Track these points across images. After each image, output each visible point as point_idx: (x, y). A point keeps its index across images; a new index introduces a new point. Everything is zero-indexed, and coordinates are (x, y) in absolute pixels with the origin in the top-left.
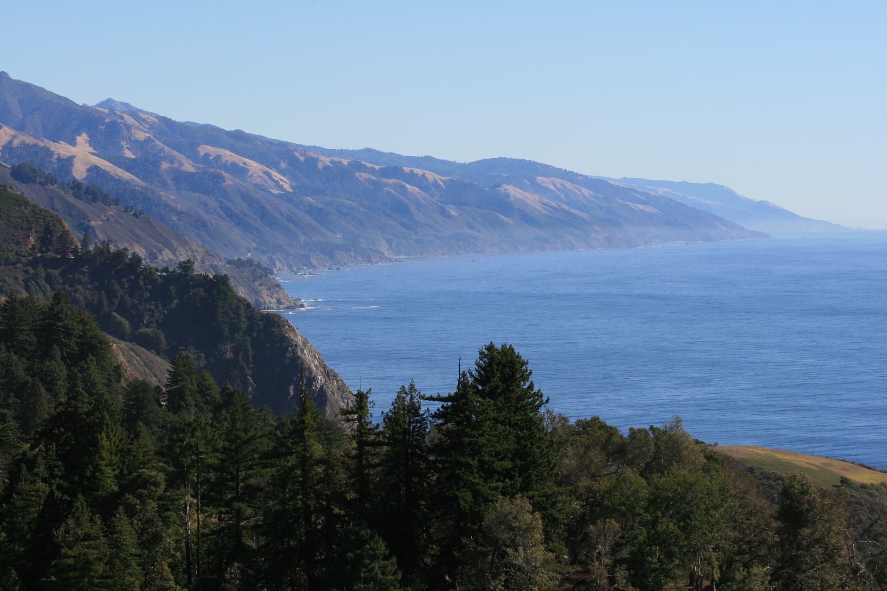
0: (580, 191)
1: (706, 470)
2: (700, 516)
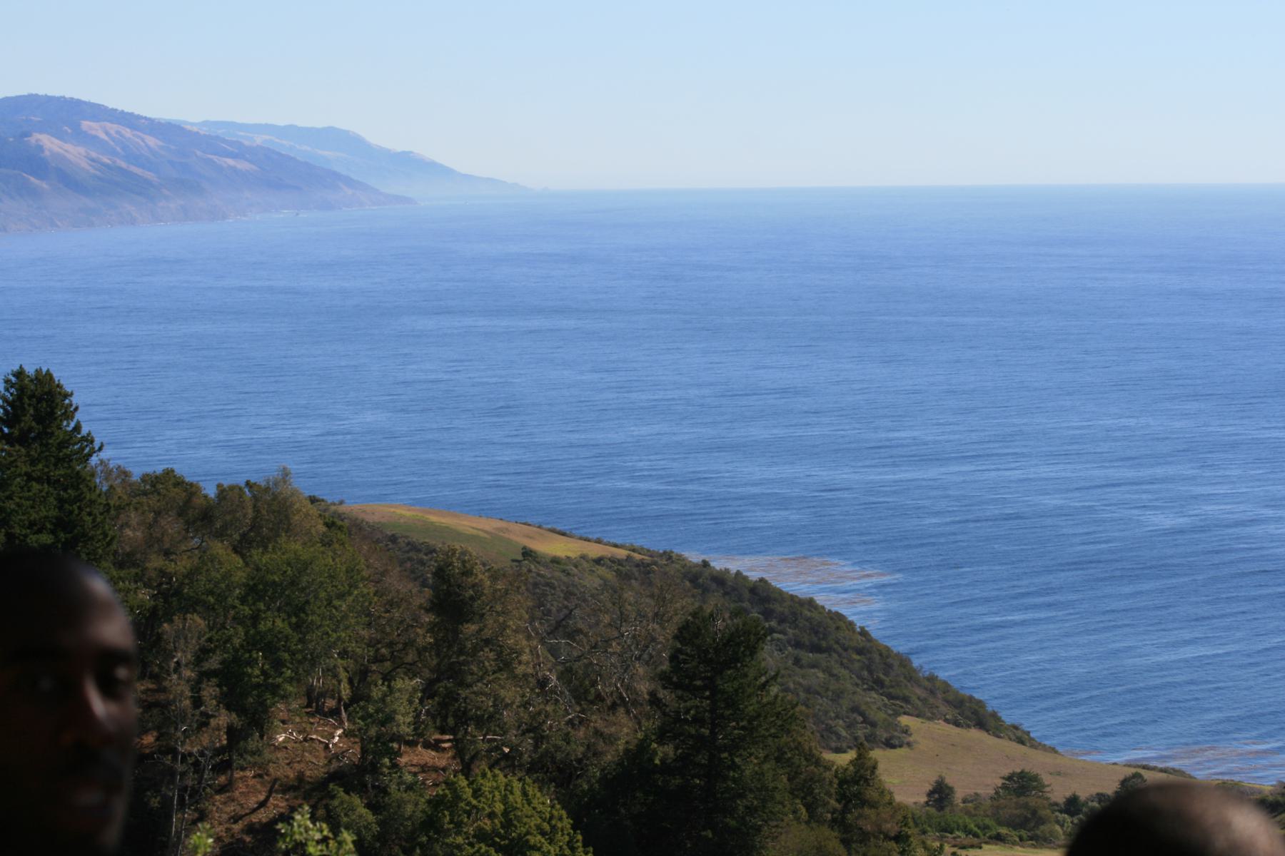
0: (143, 140)
1: (327, 543)
2: (319, 608)
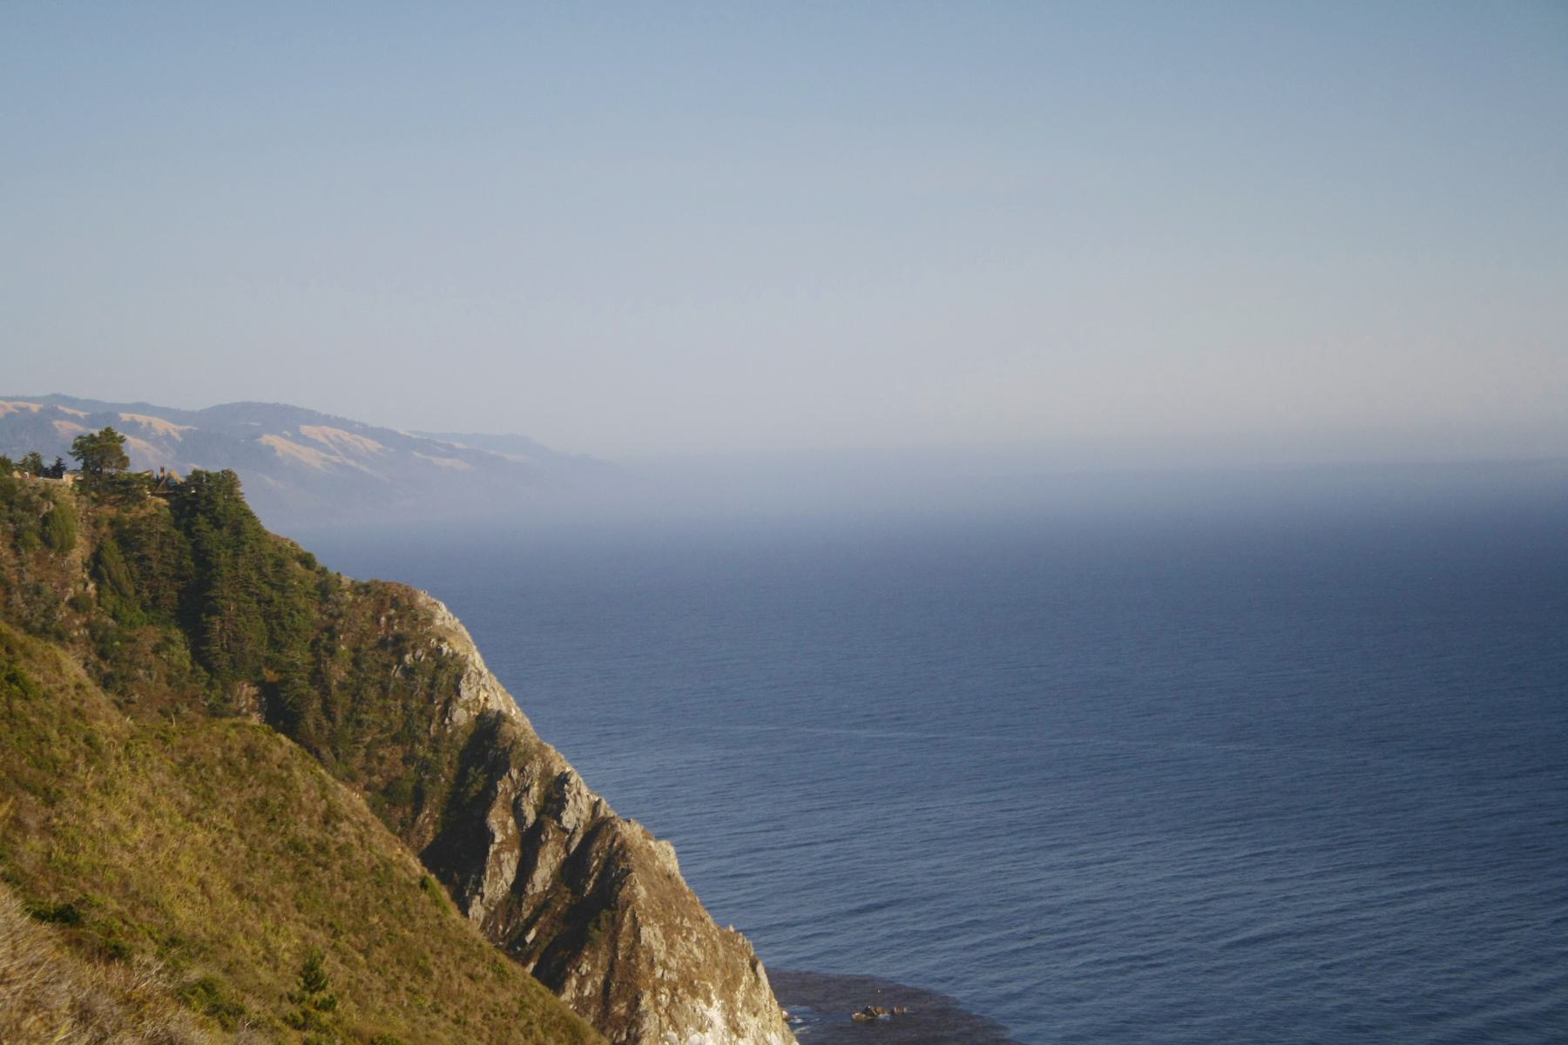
0: (362, 443)
